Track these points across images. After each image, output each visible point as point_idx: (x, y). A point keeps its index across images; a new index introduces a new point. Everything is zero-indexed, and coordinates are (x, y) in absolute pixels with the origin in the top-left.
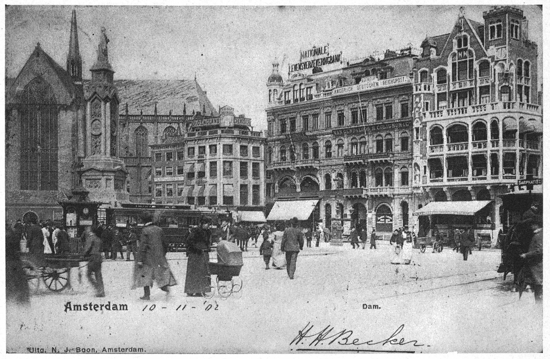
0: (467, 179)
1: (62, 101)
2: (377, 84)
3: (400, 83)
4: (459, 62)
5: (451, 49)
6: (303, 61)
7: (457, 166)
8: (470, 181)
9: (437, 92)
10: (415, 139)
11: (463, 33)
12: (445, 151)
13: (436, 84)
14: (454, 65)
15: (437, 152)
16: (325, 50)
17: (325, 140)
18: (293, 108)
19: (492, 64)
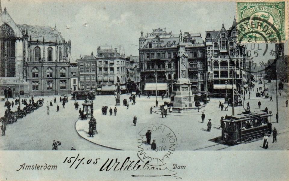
0: (228, 78)
1: (18, 36)
2: (192, 45)
3: (200, 46)
4: (222, 41)
5: (220, 37)
6: (154, 33)
7: (224, 74)
8: (220, 78)
9: (214, 49)
10: (208, 65)
11: (224, 33)
12: (220, 69)
13: (214, 47)
14: (220, 42)
15: (216, 69)
16: (164, 30)
17: (168, 62)
18: (160, 49)
19: (234, 43)
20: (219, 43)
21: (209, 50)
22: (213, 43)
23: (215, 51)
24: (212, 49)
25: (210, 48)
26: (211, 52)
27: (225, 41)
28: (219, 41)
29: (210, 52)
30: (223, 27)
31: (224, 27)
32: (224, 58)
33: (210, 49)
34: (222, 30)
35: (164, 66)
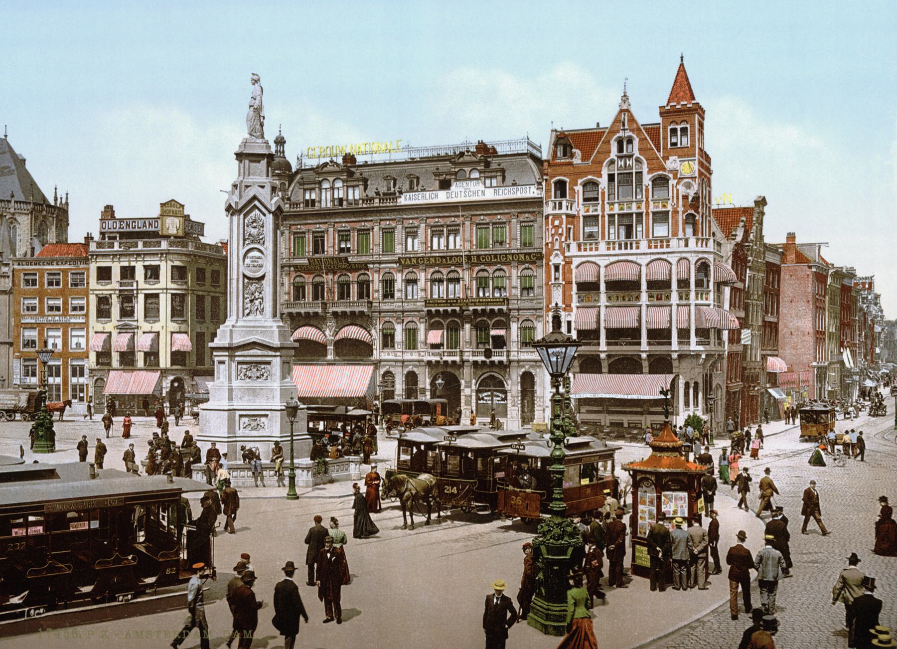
9: (582, 213)
11: (629, 133)
14: (611, 178)
20: (603, 181)
21: (556, 216)
22: (580, 181)
23: (584, 217)
24: (574, 212)
25: (560, 208)
26: (564, 226)
27: (634, 171)
28: (605, 173)
29: (561, 223)
30: (625, 107)
31: (628, 111)
32: (623, 251)
33: (564, 210)
34: (617, 121)
35: (364, 289)
